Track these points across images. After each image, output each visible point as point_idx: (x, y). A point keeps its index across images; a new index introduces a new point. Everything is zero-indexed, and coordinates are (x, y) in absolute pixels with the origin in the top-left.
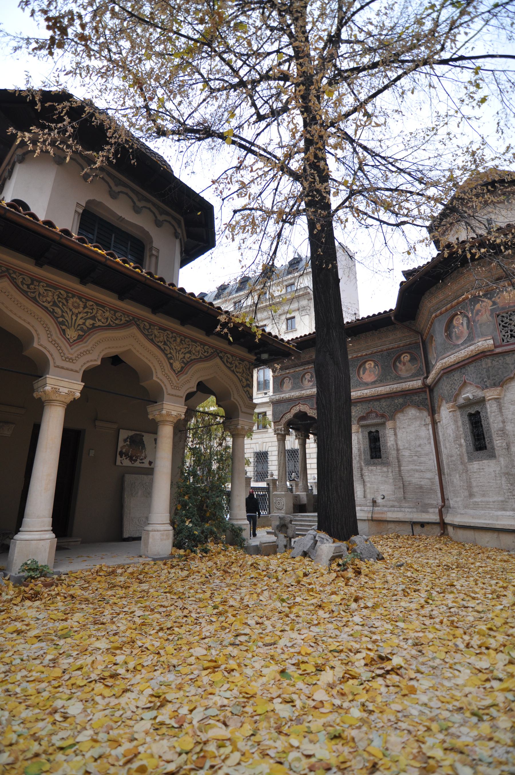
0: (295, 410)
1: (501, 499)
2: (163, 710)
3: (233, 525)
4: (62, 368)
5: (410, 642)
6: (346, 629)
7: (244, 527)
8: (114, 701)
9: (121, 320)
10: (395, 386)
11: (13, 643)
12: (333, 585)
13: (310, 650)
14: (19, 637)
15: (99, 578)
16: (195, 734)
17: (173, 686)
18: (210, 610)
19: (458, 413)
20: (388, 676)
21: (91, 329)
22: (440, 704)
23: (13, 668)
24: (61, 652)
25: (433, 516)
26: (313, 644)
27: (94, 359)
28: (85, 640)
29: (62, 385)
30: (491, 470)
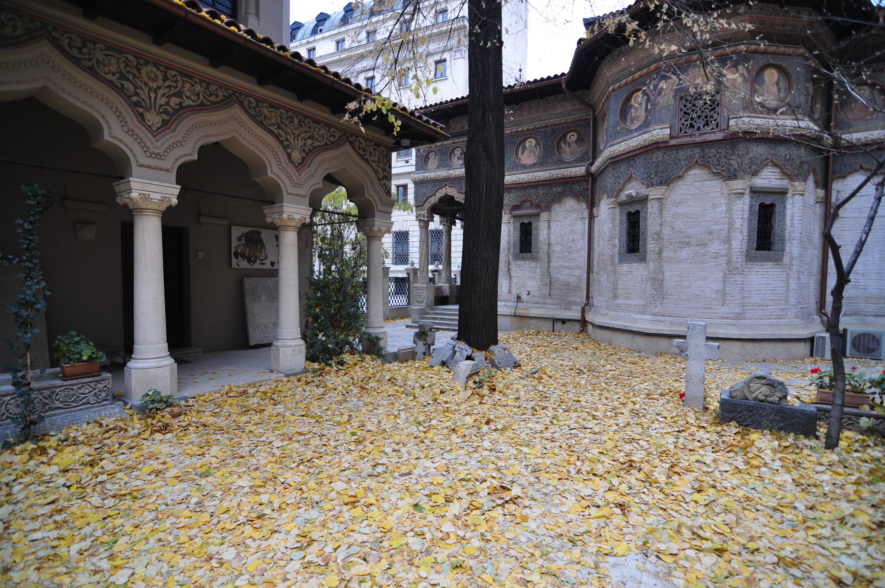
0: (441, 193)
1: (643, 302)
2: (309, 550)
3: (369, 335)
4: (149, 167)
5: (530, 468)
6: (476, 455)
7: (381, 336)
8: (264, 544)
9: (217, 96)
10: (556, 172)
11: (153, 486)
12: (467, 403)
13: (440, 479)
14: (158, 479)
15: (230, 401)
16: (340, 572)
17: (317, 523)
18: (349, 437)
19: (618, 210)
20: (506, 506)
21: (178, 110)
22: (545, 531)
23: (160, 516)
24: (205, 493)
25: (575, 314)
26: (444, 473)
27: (189, 152)
28: (227, 478)
29: (152, 190)
30: (639, 274)
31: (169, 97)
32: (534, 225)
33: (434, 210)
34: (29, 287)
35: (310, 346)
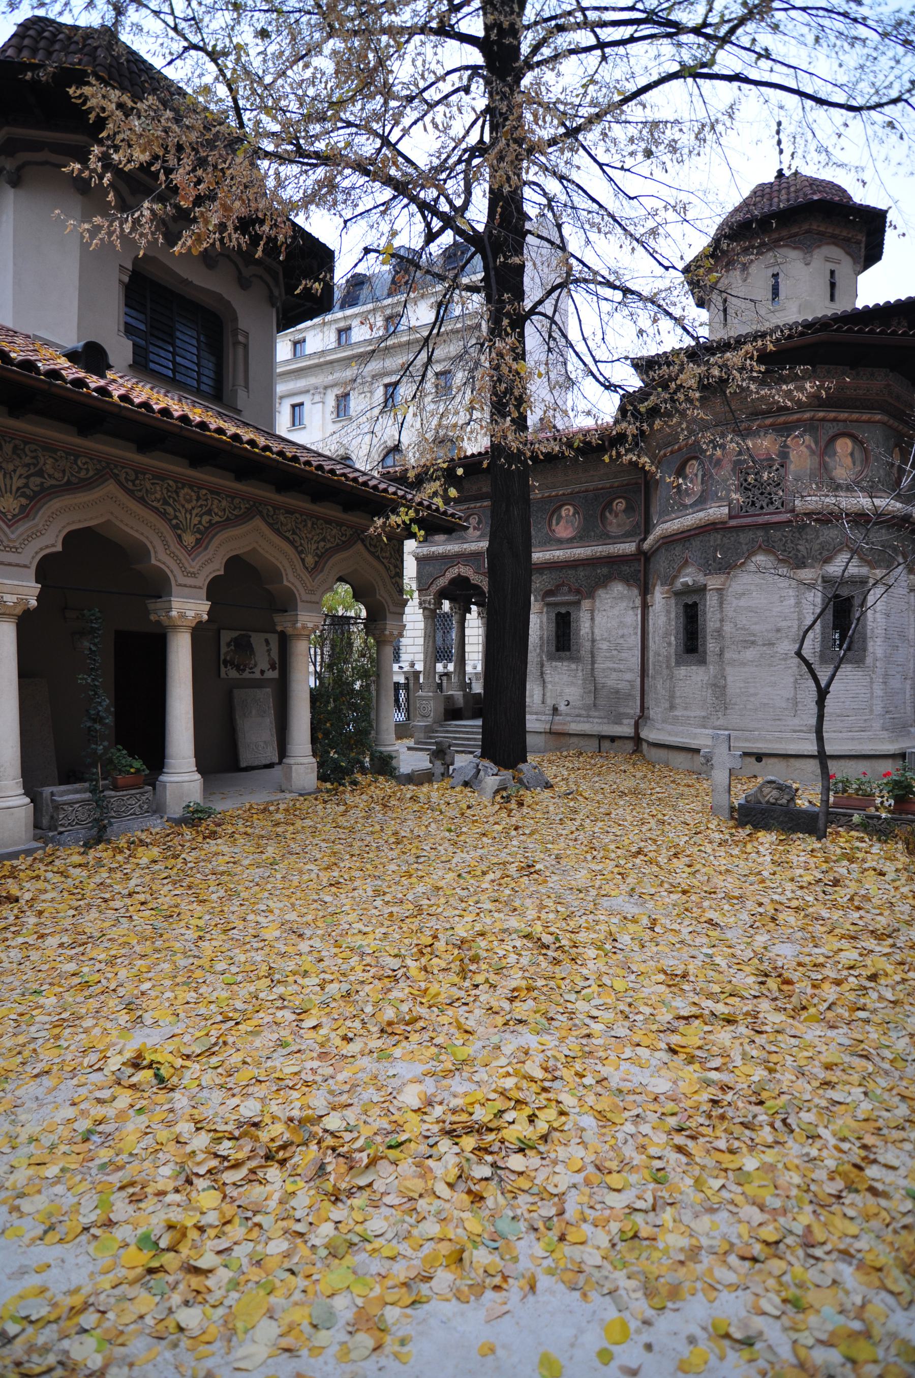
10: (600, 548)
19: (673, 601)
25: (626, 729)
27: (217, 568)
29: (188, 607)
32: (573, 616)
33: (442, 594)
35: (320, 765)
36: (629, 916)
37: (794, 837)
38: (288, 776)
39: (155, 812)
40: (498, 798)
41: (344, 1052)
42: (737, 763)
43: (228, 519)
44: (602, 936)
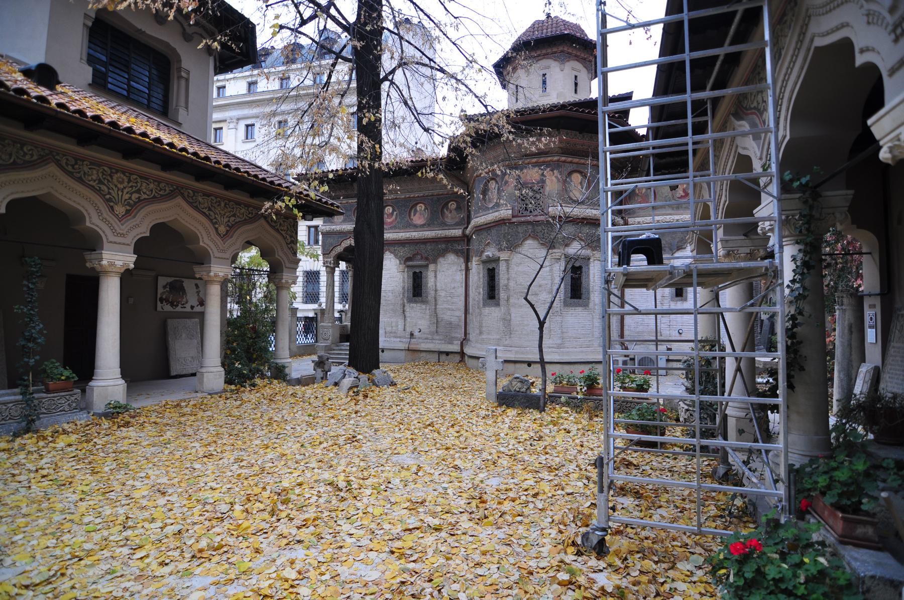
4: (115, 243)
7: (286, 365)
10: (440, 232)
19: (481, 267)
25: (456, 347)
27: (144, 230)
29: (117, 258)
31: (131, 194)
33: (340, 257)
34: (34, 328)
35: (228, 372)
36: (405, 466)
37: (527, 411)
38: (201, 382)
39: (82, 410)
40: (351, 393)
41: (156, 574)
42: (500, 367)
43: (154, 197)
44: (381, 481)
